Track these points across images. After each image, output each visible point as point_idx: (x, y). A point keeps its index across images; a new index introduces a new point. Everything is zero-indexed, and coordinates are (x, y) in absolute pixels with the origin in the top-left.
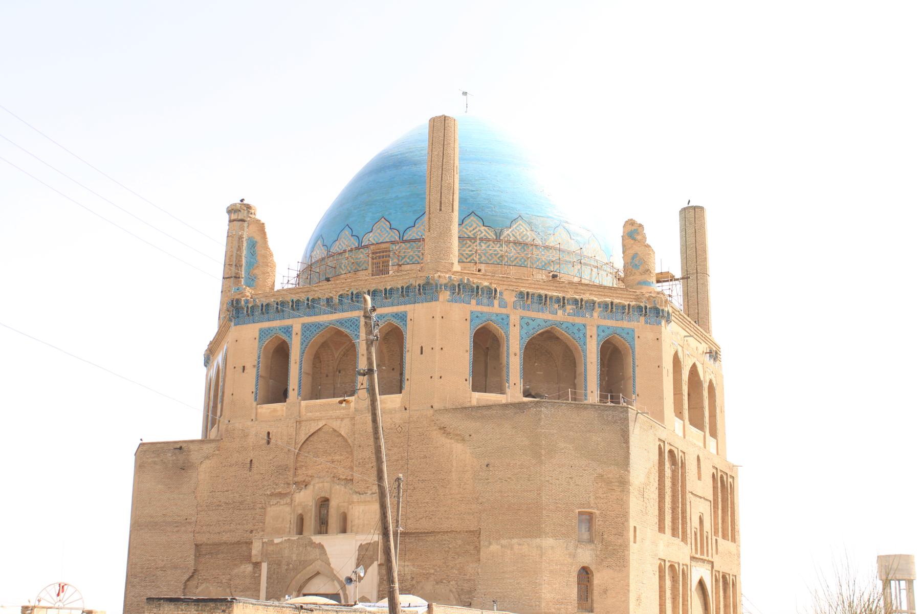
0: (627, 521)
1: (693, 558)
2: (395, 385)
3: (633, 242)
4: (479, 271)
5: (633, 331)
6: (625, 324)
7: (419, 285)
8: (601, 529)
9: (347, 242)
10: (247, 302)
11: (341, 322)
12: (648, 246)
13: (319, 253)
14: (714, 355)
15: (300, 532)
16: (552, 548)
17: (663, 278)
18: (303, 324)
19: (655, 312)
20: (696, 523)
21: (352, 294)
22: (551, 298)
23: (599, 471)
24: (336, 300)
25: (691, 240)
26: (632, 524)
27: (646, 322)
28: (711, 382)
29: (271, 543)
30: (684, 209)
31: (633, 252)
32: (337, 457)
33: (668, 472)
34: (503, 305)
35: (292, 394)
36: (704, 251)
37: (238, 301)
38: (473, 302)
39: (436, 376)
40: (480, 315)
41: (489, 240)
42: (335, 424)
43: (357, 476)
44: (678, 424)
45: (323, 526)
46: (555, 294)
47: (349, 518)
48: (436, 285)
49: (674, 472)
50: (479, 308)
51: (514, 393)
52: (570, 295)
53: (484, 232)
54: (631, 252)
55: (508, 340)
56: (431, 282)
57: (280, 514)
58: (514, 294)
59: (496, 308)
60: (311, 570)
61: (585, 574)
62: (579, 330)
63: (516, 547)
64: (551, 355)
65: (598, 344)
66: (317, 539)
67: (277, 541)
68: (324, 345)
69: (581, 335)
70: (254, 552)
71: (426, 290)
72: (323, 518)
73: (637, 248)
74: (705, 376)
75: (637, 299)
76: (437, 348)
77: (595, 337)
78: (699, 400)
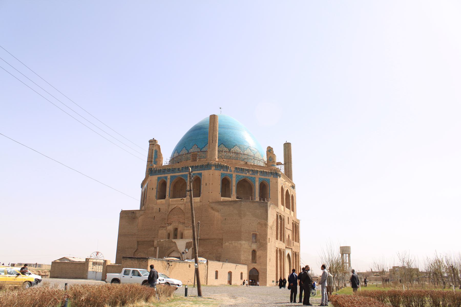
0: (267, 236)
1: (286, 247)
2: (198, 194)
6: (267, 177)
8: (259, 239)
9: (184, 152)
10: (154, 169)
11: (182, 175)
13: (176, 155)
14: (293, 187)
15: (169, 238)
17: (279, 164)
19: (276, 174)
20: (287, 237)
23: (259, 221)
25: (287, 153)
26: (268, 237)
29: (160, 241)
30: (285, 144)
32: (180, 216)
33: (279, 222)
34: (231, 171)
35: (167, 197)
36: (291, 156)
37: (151, 169)
38: (222, 170)
39: (210, 192)
42: (180, 206)
43: (186, 222)
44: (282, 207)
45: (175, 237)
47: (183, 234)
49: (281, 222)
50: (224, 172)
51: (233, 197)
52: (251, 168)
53: (225, 149)
57: (163, 232)
60: (172, 249)
61: (254, 252)
63: (233, 244)
64: (245, 187)
66: (174, 240)
67: (162, 241)
68: (177, 182)
70: (155, 244)
71: (208, 166)
72: (176, 234)
73: (271, 155)
74: (290, 193)
75: (271, 170)
76: (211, 184)
78: (289, 201)
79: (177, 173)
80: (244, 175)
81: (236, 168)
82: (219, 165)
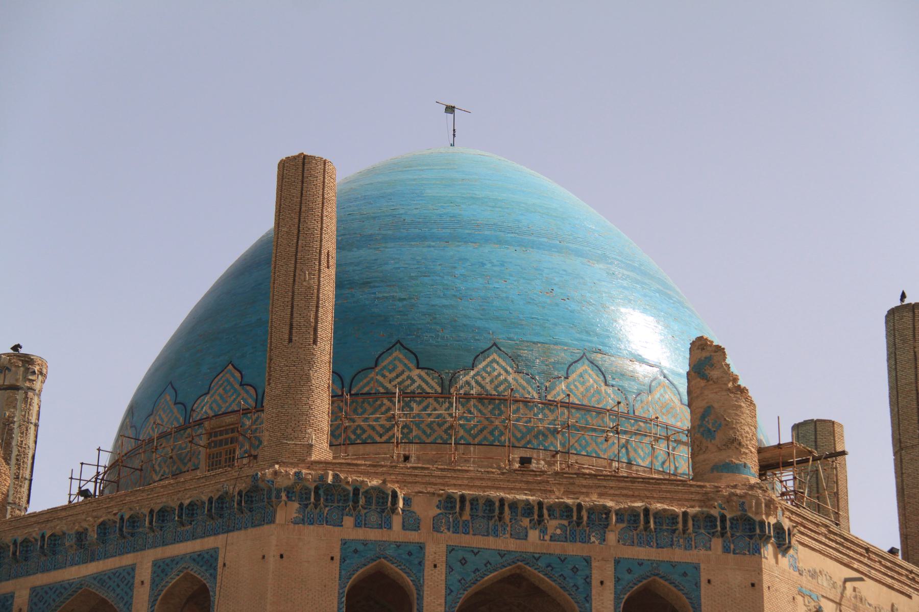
3: (703, 383)
4: (406, 458)
5: (697, 568)
6: (678, 555)
7: (240, 493)
9: (170, 417)
11: (100, 578)
12: (742, 391)
13: (129, 445)
18: (33, 590)
21: (122, 518)
22: (514, 505)
24: (93, 535)
27: (726, 550)
31: (704, 404)
38: (348, 521)
40: (360, 547)
41: (427, 396)
46: (524, 497)
48: (270, 490)
50: (361, 534)
53: (418, 379)
54: (701, 404)
55: (420, 598)
56: (261, 485)
58: (436, 500)
59: (397, 532)
62: (575, 570)
65: (617, 598)
69: (580, 582)
71: (252, 505)
75: (706, 500)
77: (610, 584)
79: (73, 564)
80: (507, 543)
81: (450, 498)
82: (329, 489)
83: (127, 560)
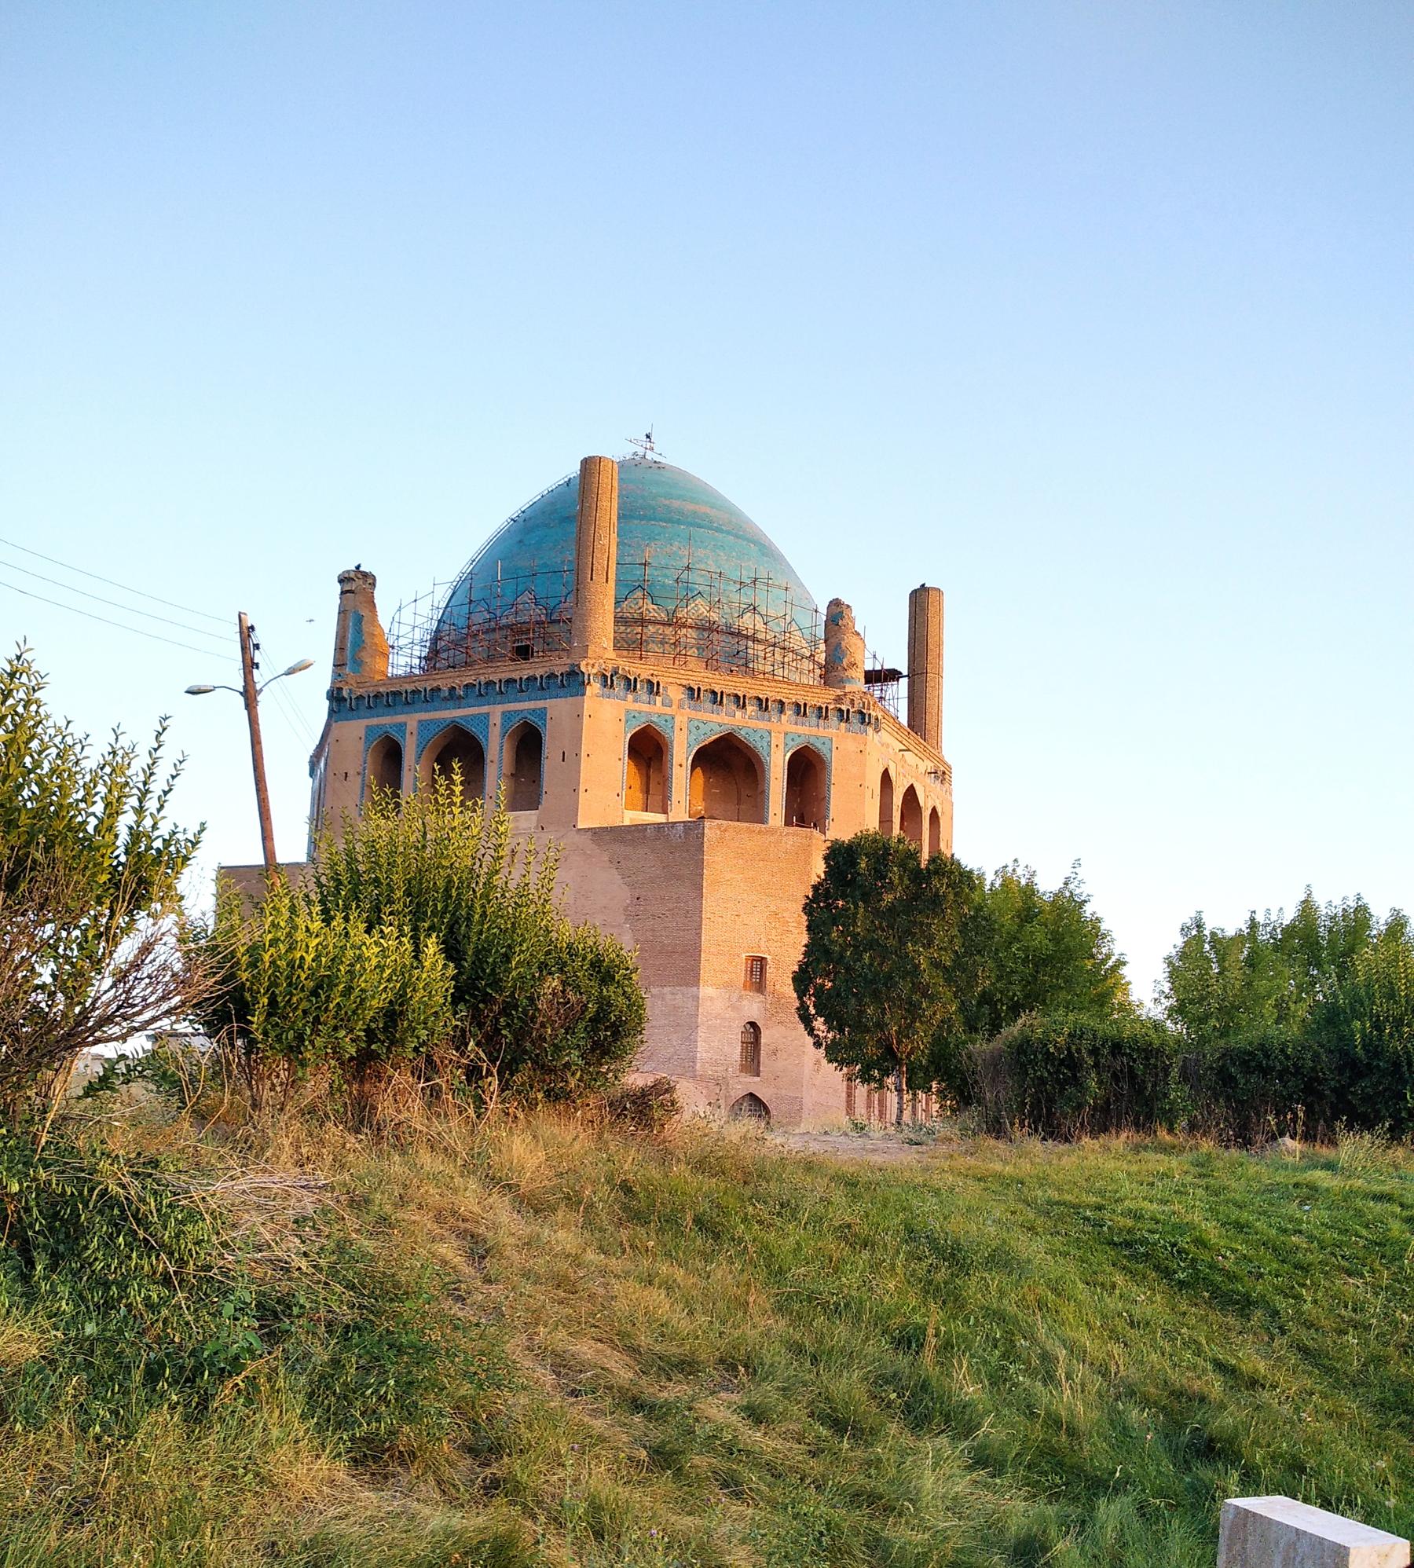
14: (942, 775)
16: (712, 999)
17: (880, 677)
23: (773, 908)
28: (934, 810)
50: (637, 706)
62: (762, 737)
74: (926, 802)
83: (485, 709)
